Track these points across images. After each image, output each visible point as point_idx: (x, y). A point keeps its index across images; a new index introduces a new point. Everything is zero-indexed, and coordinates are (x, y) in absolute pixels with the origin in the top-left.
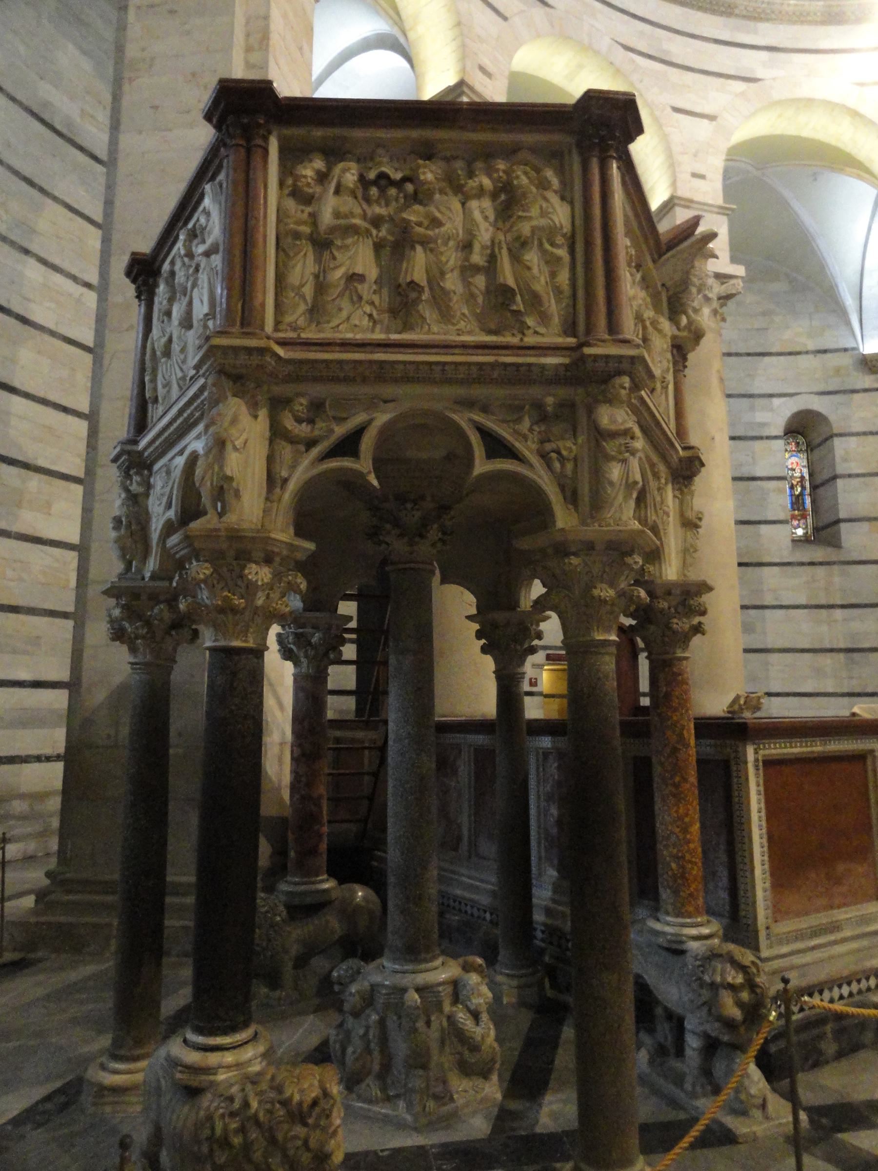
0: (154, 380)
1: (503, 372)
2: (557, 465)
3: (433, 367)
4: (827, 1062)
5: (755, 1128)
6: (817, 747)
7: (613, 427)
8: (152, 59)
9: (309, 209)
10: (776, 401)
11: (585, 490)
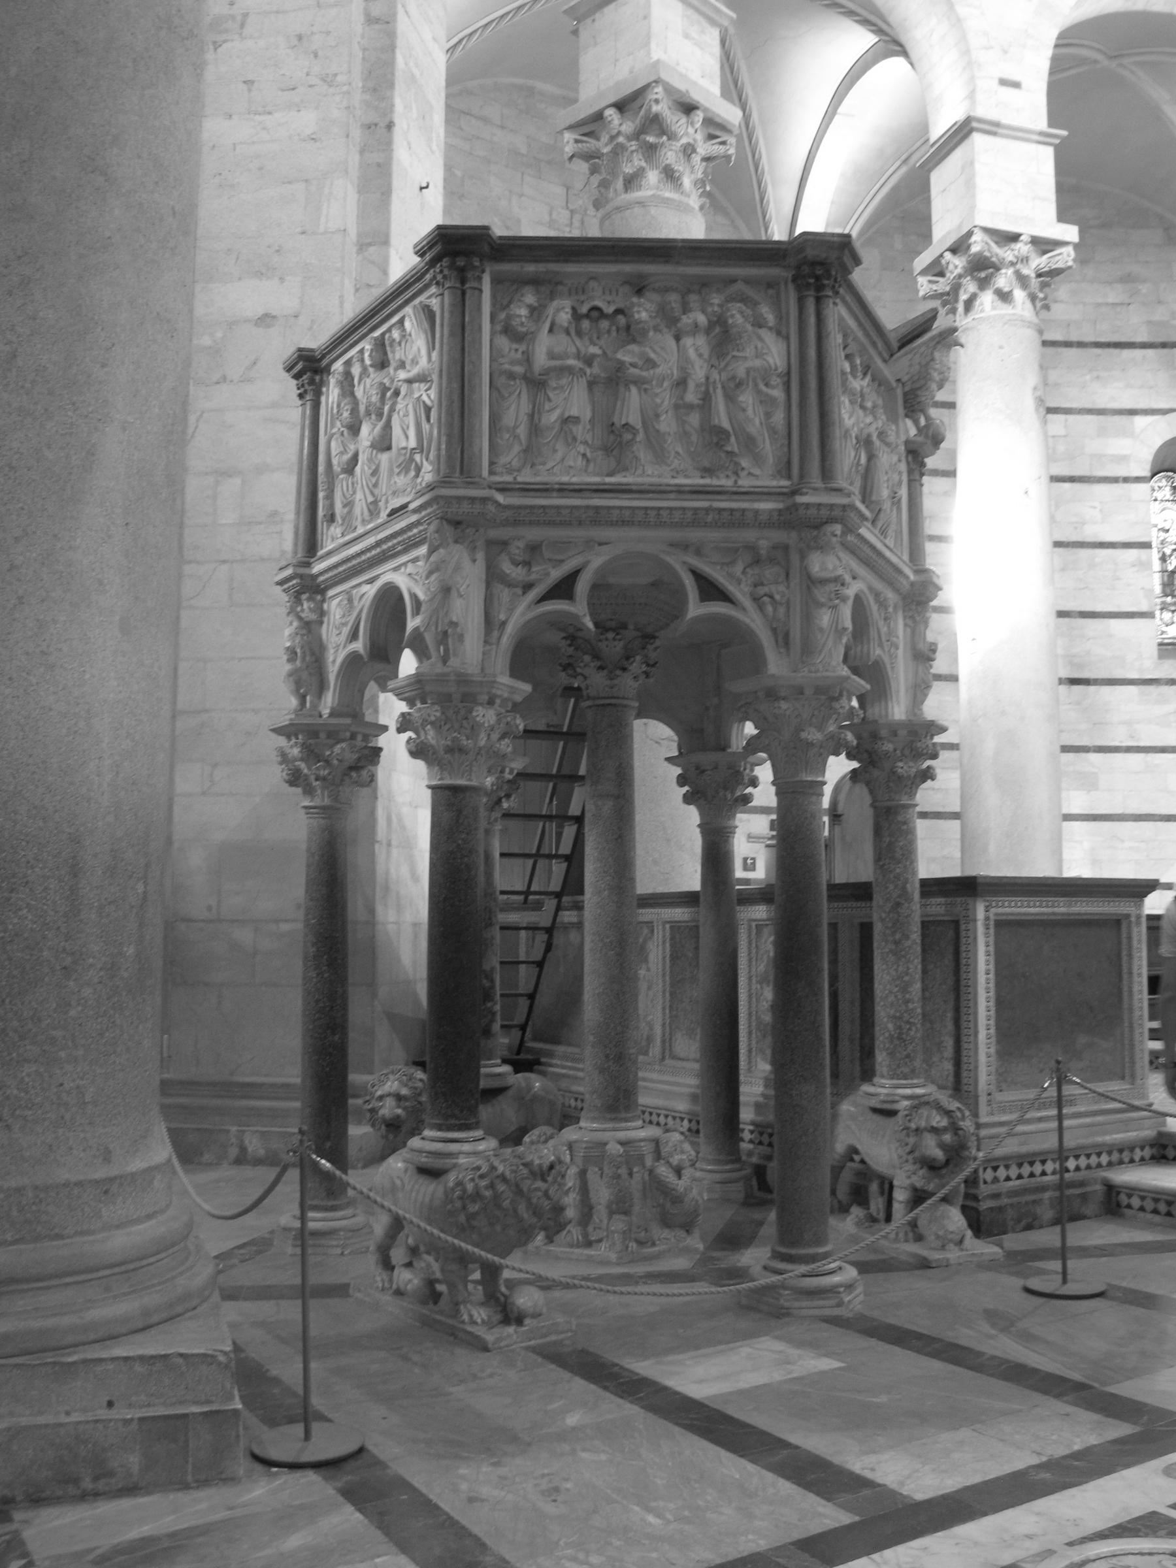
0: (330, 497)
2: (770, 609)
4: (1041, 1227)
5: (949, 1255)
6: (1061, 908)
7: (825, 575)
8: (246, 15)
9: (523, 348)
10: (1140, 421)
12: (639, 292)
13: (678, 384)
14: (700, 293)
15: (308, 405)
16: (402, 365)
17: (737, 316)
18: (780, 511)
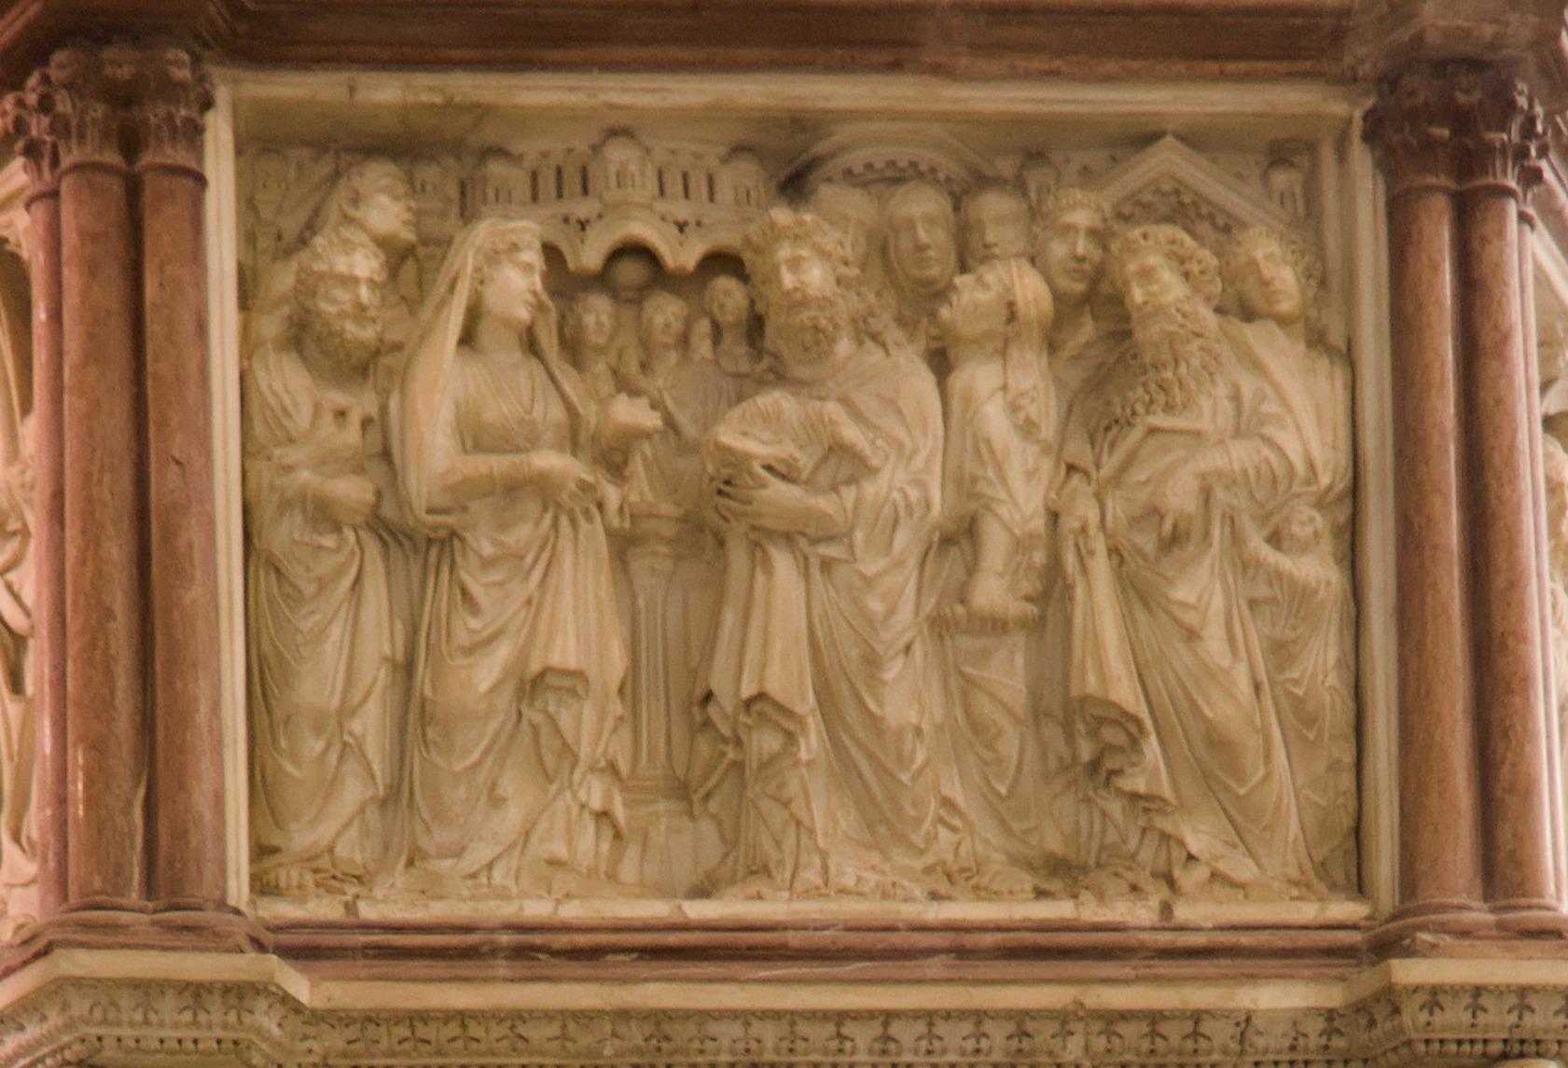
1: (1100, 1043)
9: (362, 403)
13: (947, 541)
14: (1020, 186)
17: (1162, 279)
18: (1330, 1015)
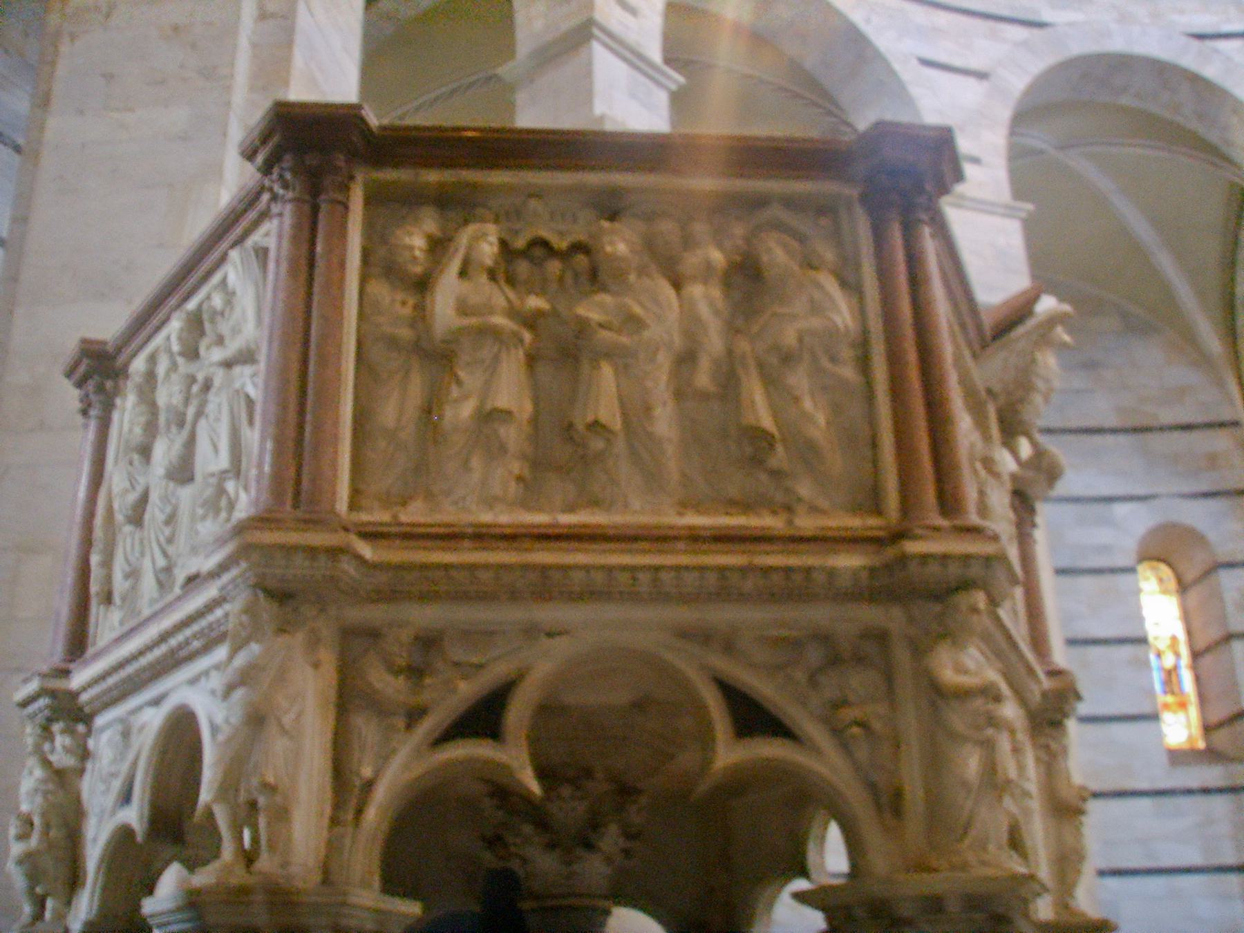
0: (107, 563)
3: (641, 576)
11: (914, 794)
12: (613, 216)
15: (93, 425)
16: (220, 341)
17: (776, 254)
